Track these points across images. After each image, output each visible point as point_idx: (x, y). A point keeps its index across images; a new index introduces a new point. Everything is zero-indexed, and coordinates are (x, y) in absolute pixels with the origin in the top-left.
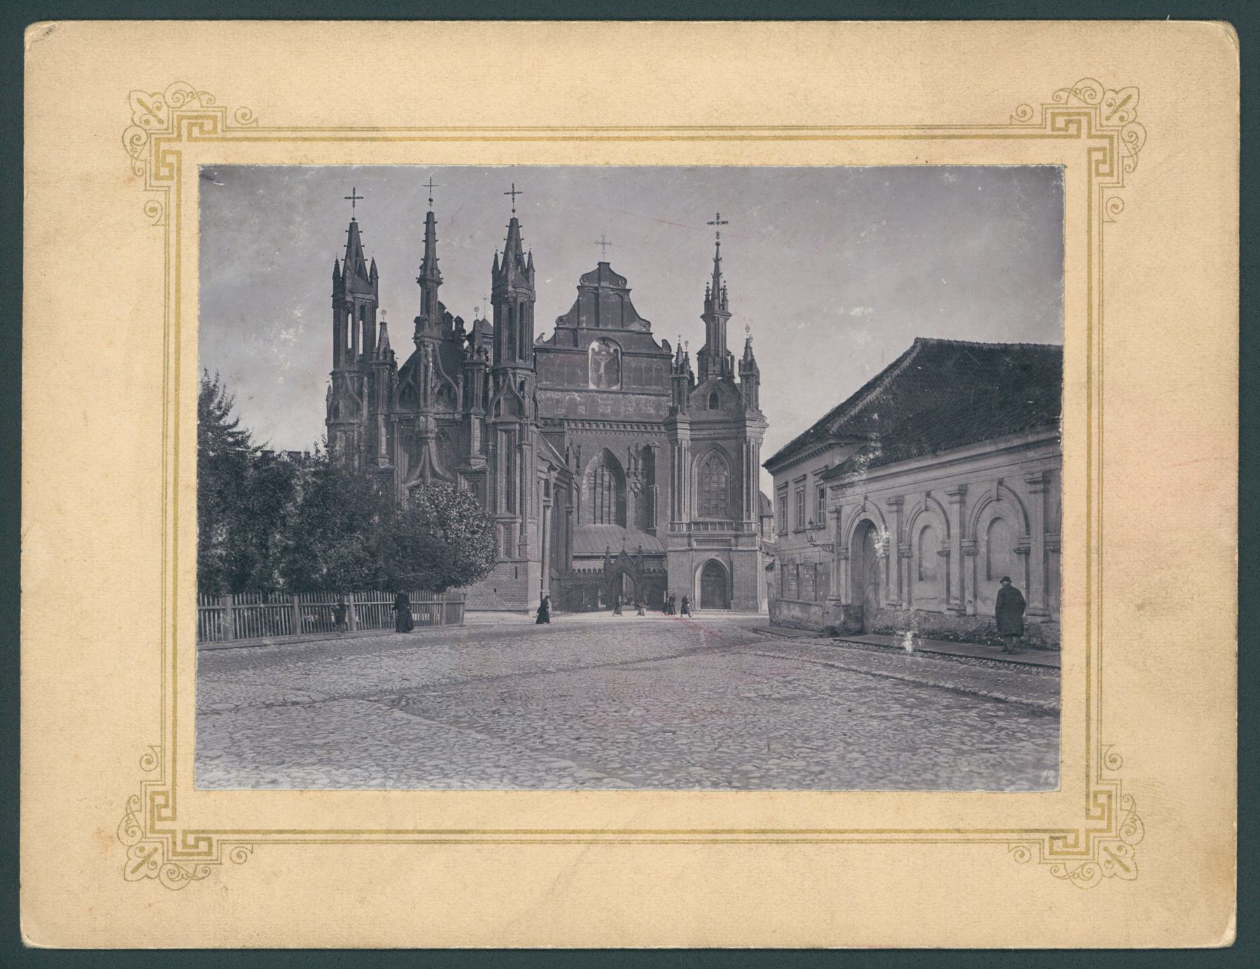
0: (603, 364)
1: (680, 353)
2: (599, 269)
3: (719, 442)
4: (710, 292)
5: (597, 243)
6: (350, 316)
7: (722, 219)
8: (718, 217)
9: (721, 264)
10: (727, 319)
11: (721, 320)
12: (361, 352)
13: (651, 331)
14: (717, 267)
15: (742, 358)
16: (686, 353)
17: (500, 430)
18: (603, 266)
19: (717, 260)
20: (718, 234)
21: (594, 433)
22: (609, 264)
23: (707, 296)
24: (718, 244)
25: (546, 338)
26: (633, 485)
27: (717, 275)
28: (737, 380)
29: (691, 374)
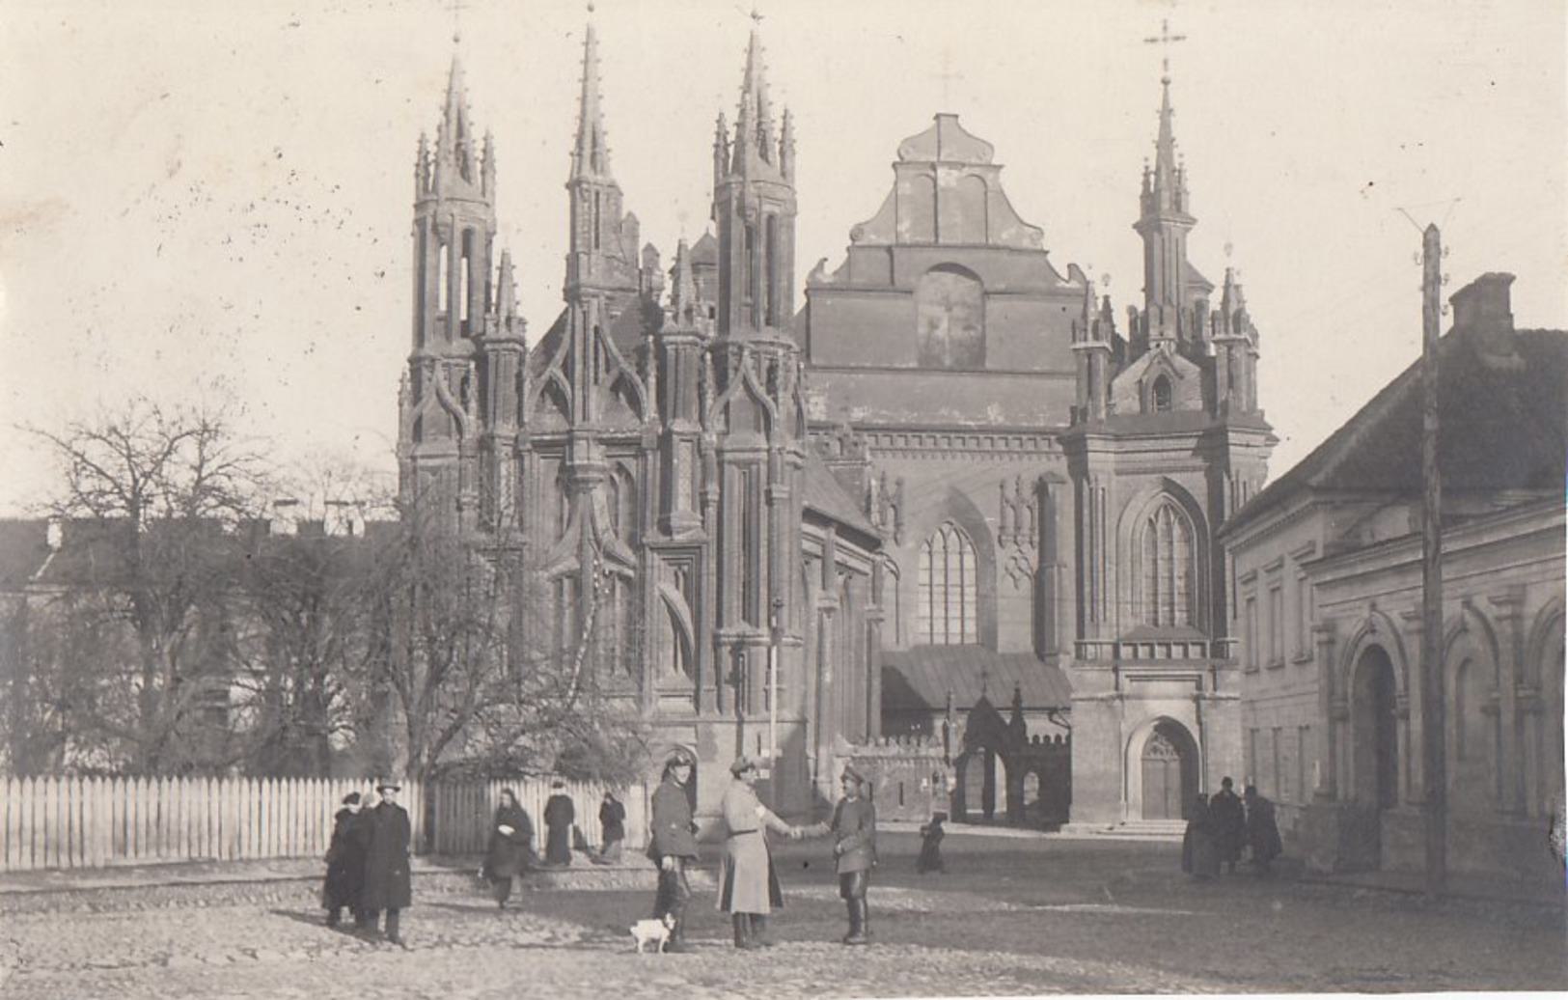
3: (1169, 476)
4: (1152, 178)
8: (1165, 28)
10: (1188, 230)
11: (1176, 231)
12: (464, 317)
13: (1046, 245)
14: (1165, 126)
16: (1106, 298)
17: (730, 462)
19: (1166, 113)
20: (1165, 62)
22: (956, 116)
23: (1146, 183)
24: (1166, 82)
25: (830, 268)
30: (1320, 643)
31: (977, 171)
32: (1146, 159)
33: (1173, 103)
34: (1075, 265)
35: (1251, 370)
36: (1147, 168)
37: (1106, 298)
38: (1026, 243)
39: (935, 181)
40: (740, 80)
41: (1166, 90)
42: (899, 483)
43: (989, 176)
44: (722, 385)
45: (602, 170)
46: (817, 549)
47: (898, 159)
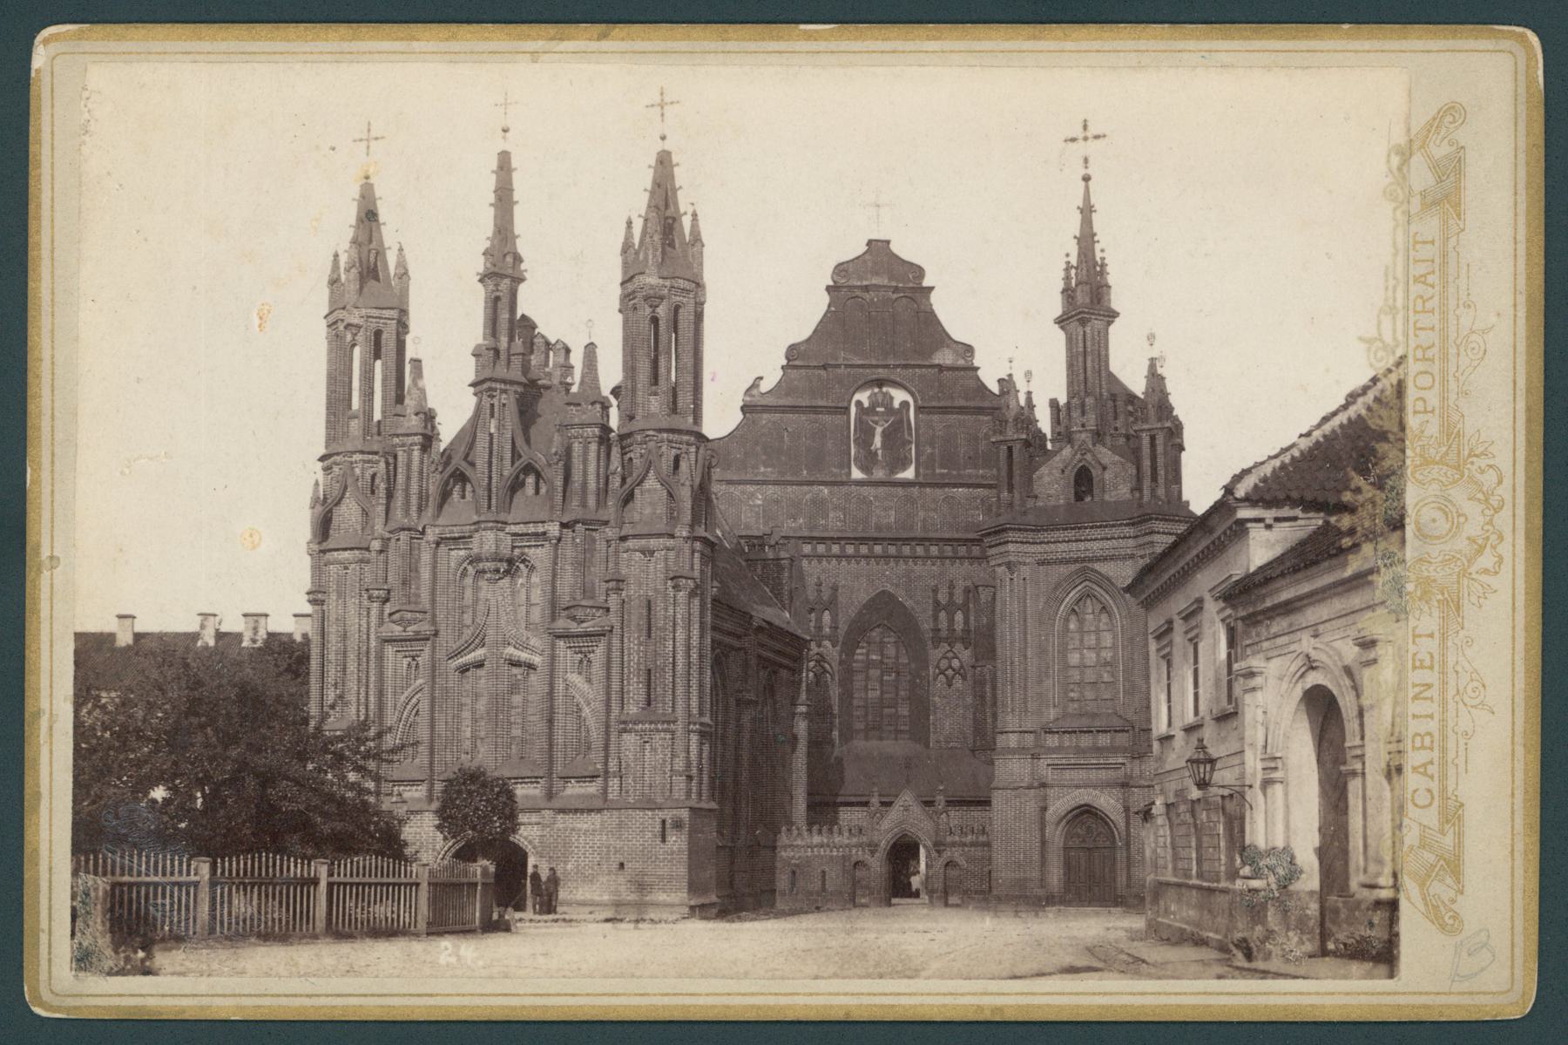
0: (879, 430)
3: (1097, 566)
7: (1092, 131)
8: (1085, 127)
9: (1096, 219)
13: (976, 363)
16: (1029, 393)
18: (878, 249)
19: (1087, 211)
20: (1086, 160)
21: (863, 562)
22: (888, 242)
23: (1067, 278)
24: (1087, 179)
25: (765, 386)
27: (1087, 240)
32: (1067, 255)
33: (1093, 201)
36: (1068, 263)
37: (1029, 393)
41: (1087, 189)
42: (835, 589)
47: (831, 283)
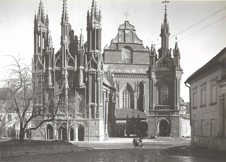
1: (152, 47)
2: (125, 23)
3: (166, 79)
4: (163, 26)
5: (124, 15)
6: (40, 36)
11: (167, 36)
13: (143, 43)
15: (174, 49)
17: (90, 74)
19: (166, 15)
20: (166, 6)
22: (128, 21)
23: (162, 27)
24: (166, 10)
25: (108, 46)
26: (137, 95)
27: (165, 20)
28: (173, 57)
29: (156, 55)
30: (220, 99)
31: (132, 31)
32: (162, 23)
34: (147, 47)
35: (179, 60)
38: (140, 43)
39: (125, 32)
40: (91, 5)
41: (166, 11)
42: (119, 82)
43: (134, 32)
44: (88, 61)
45: (67, 21)
46: (105, 91)
